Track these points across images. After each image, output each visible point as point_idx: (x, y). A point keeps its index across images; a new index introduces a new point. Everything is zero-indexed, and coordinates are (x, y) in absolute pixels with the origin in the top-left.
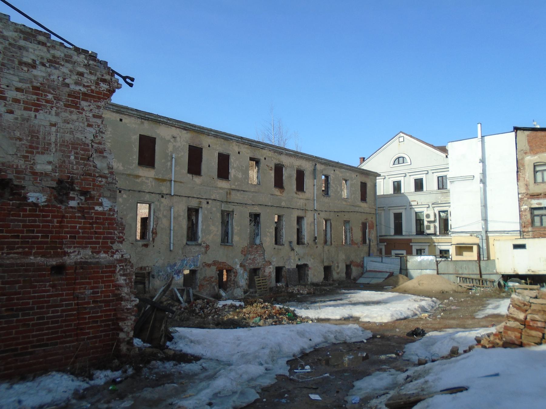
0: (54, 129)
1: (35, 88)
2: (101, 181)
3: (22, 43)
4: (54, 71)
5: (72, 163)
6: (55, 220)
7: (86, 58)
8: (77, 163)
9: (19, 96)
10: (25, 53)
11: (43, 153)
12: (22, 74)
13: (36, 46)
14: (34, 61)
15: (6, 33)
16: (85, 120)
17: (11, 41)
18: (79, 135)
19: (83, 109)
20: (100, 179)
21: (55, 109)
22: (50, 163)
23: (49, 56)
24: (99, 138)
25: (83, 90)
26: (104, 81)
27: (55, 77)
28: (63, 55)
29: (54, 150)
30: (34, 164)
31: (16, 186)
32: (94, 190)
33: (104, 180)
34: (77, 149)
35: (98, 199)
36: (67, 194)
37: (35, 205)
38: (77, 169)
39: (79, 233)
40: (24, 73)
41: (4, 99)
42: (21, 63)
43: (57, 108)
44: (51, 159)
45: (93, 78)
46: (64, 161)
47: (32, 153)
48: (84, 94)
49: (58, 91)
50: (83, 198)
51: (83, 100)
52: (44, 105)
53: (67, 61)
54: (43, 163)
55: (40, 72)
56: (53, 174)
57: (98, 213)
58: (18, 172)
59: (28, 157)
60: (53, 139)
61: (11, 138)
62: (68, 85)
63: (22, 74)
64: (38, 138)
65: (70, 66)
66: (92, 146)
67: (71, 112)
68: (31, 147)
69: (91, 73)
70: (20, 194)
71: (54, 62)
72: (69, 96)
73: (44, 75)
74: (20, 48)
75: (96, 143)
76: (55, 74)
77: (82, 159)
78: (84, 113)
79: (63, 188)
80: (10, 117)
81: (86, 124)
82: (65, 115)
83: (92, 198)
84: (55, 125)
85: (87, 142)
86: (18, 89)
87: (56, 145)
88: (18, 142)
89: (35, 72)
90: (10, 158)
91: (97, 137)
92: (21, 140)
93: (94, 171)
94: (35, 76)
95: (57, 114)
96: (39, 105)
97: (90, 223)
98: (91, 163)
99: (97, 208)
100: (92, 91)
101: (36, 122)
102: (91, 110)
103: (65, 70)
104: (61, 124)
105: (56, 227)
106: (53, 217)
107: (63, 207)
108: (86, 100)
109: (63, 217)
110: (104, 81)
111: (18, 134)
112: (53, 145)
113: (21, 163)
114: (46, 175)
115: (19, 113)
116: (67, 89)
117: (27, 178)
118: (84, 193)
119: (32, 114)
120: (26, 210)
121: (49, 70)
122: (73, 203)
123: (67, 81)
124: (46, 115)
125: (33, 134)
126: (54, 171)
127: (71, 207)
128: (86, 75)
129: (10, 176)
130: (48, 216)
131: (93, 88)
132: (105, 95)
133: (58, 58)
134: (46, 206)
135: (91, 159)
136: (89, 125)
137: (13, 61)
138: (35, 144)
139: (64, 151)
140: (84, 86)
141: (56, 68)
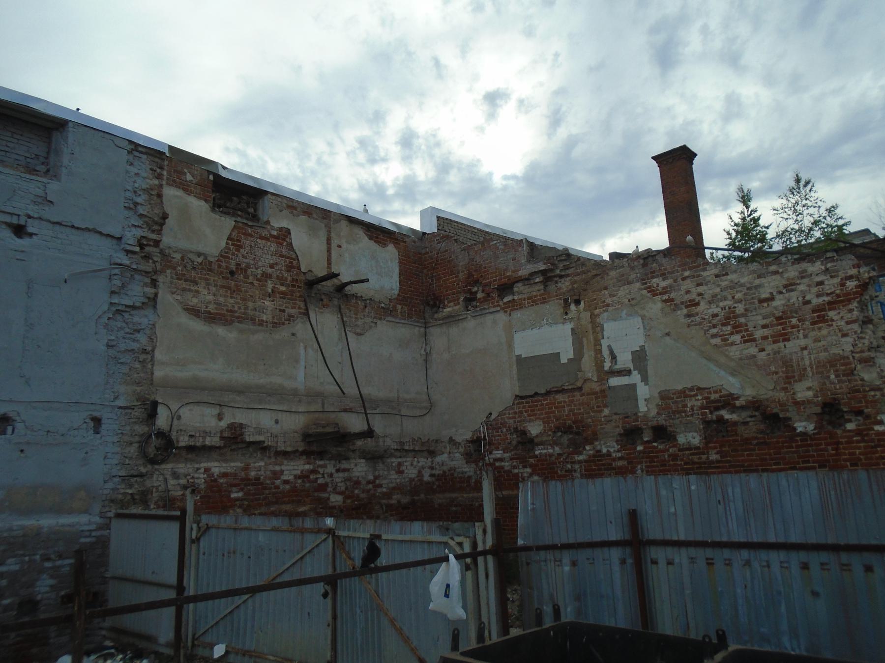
0: (806, 352)
1: (779, 318)
2: (874, 396)
3: (757, 282)
4: (792, 294)
5: (833, 383)
6: (830, 448)
7: (822, 264)
8: (839, 382)
9: (766, 332)
10: (762, 290)
11: (800, 380)
12: (764, 311)
13: (769, 279)
14: (771, 293)
15: (742, 281)
16: (837, 331)
17: (749, 285)
18: (835, 351)
19: (832, 320)
20: (872, 393)
21: (802, 331)
22: (809, 389)
23: (785, 282)
24: (860, 345)
25: (827, 299)
26: (850, 277)
27: (794, 300)
28: (797, 273)
29: (811, 374)
30: (794, 394)
31: (784, 418)
32: (867, 407)
33: (878, 393)
34: (835, 366)
35: (875, 418)
36: (843, 416)
37: (804, 434)
38: (841, 388)
39: (860, 459)
40: (766, 309)
41: (754, 340)
42: (761, 301)
43: (804, 330)
44: (810, 384)
45: (836, 281)
46: (824, 384)
47: (790, 383)
48: (829, 303)
49: (800, 313)
50: (860, 418)
51: (830, 310)
52: (791, 332)
53: (802, 277)
54: (804, 391)
55: (778, 302)
56: (815, 400)
57: (878, 433)
58: (781, 405)
59: (787, 388)
60: (807, 363)
61: (768, 374)
62: (809, 302)
63: (764, 311)
64: (792, 366)
65: (806, 280)
66: (853, 357)
67: (820, 329)
68: (787, 377)
69: (832, 277)
70: (789, 426)
71: (790, 286)
72: (814, 311)
73: (783, 302)
74: (757, 287)
75: (857, 353)
76: (794, 297)
77: (844, 375)
78: (834, 324)
79: (830, 411)
80: (763, 353)
81: (840, 335)
82: (812, 334)
83: (868, 417)
84: (805, 348)
85: (846, 354)
86: (764, 327)
87: (812, 368)
88: (775, 377)
89: (775, 303)
90: (771, 393)
91: (856, 345)
92: (776, 373)
93: (863, 386)
94: (776, 308)
95: (805, 336)
96: (786, 334)
97: (872, 447)
98: (857, 377)
99: (877, 428)
100: (838, 296)
101: (787, 351)
102: (842, 317)
103: (802, 287)
104: (811, 345)
105: (833, 455)
106: (827, 444)
107: (839, 432)
108: (834, 309)
109: (838, 443)
110: (850, 277)
111: (773, 368)
112: (809, 369)
113: (782, 396)
114: (809, 402)
115: (769, 348)
116: (809, 306)
117: (791, 409)
118: (859, 413)
119: (781, 344)
120: (797, 441)
121: (787, 295)
122: (850, 426)
123: (808, 298)
124: (795, 341)
125: (787, 363)
126: (816, 396)
127: (850, 431)
128: (826, 282)
129: (775, 411)
130: (821, 444)
131: (838, 292)
132: (855, 293)
133: (793, 279)
134: (818, 433)
135: (856, 372)
136: (845, 335)
137: (754, 303)
138: (791, 374)
139: (822, 373)
140: (828, 295)
141: (793, 290)
